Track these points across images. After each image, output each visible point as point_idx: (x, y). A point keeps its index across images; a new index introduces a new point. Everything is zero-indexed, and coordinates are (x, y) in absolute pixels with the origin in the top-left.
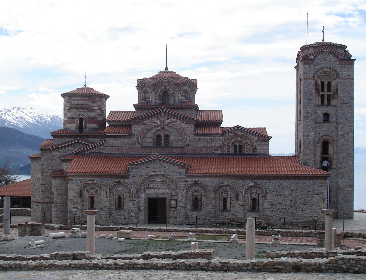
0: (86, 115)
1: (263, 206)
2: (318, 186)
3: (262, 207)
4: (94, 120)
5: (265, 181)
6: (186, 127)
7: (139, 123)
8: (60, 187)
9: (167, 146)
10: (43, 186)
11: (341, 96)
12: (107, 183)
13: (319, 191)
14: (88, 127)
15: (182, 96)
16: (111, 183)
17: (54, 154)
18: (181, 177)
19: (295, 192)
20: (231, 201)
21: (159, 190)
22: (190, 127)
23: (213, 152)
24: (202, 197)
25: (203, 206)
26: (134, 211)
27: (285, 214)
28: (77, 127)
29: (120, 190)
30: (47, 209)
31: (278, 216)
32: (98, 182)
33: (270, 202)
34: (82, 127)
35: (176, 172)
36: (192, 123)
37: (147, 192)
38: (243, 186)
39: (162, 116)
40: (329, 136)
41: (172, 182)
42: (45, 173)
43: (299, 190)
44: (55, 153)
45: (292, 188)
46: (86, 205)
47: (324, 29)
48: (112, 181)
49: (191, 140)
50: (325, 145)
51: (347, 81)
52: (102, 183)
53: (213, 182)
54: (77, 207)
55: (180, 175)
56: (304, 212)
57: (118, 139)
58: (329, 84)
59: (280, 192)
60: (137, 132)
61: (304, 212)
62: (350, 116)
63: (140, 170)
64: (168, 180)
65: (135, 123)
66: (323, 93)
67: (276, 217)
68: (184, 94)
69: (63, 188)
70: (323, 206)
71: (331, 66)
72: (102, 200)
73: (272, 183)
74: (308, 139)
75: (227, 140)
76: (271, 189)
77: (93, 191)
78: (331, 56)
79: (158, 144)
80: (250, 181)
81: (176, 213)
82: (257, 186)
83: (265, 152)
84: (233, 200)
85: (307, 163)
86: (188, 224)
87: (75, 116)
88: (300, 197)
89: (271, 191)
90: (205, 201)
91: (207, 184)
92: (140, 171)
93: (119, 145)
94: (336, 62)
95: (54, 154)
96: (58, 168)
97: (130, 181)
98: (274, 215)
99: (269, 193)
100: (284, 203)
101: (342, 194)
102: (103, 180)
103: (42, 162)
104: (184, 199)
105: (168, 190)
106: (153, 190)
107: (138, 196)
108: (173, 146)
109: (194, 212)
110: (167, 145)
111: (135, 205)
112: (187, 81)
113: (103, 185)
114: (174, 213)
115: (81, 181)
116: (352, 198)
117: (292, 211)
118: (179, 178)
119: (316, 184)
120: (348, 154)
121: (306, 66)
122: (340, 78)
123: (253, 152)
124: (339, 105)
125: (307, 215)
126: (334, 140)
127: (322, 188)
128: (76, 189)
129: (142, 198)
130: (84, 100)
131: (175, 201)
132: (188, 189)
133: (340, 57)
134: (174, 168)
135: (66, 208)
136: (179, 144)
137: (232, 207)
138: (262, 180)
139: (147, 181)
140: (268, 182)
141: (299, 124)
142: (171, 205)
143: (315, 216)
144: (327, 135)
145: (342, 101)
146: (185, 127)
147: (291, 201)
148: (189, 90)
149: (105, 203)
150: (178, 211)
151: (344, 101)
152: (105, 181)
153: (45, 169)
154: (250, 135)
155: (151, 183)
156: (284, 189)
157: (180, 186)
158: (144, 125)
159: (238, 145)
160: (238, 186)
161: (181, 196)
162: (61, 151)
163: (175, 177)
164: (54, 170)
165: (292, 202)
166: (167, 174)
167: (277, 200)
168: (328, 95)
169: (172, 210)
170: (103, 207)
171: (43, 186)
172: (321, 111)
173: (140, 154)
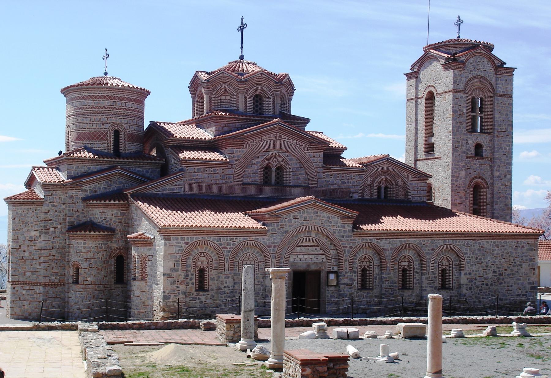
0: (125, 126)
1: (457, 281)
2: (527, 250)
3: (455, 283)
5: (462, 242)
7: (241, 145)
11: (497, 119)
12: (231, 245)
13: (529, 257)
16: (237, 244)
17: (73, 194)
18: (345, 235)
19: (500, 259)
21: (310, 257)
22: (317, 155)
23: (351, 197)
24: (374, 268)
25: (375, 282)
30: (54, 295)
31: (477, 295)
32: (215, 242)
33: (468, 274)
37: (292, 259)
38: (433, 250)
39: (276, 134)
42: (52, 229)
44: (75, 192)
45: (495, 252)
47: (459, 20)
50: (476, 189)
51: (505, 98)
52: (221, 244)
53: (391, 243)
54: (178, 289)
55: (345, 232)
57: (205, 169)
59: (480, 259)
60: (236, 158)
61: (510, 288)
62: (508, 149)
63: (284, 222)
64: (324, 240)
67: (476, 297)
69: (100, 255)
70: (533, 279)
72: (221, 275)
74: (458, 181)
75: (370, 178)
76: (470, 255)
78: (486, 60)
79: (266, 181)
80: (442, 242)
81: (335, 295)
83: (421, 199)
84: (417, 272)
87: (107, 126)
89: (469, 257)
91: (384, 246)
92: (283, 223)
93: (207, 181)
94: (491, 70)
95: (73, 193)
97: (268, 242)
98: (473, 295)
99: (467, 260)
100: (485, 276)
102: (223, 239)
103: (44, 208)
104: (350, 272)
105: (324, 256)
106: (301, 256)
108: (291, 184)
109: (362, 293)
110: (278, 183)
113: (223, 248)
114: (333, 294)
115: (186, 241)
117: (495, 288)
118: (343, 236)
119: (525, 246)
123: (405, 198)
124: (496, 133)
125: (514, 292)
128: (176, 256)
131: (335, 275)
134: (336, 219)
135: (104, 293)
136: (300, 182)
137: (416, 284)
138: (458, 241)
139: (292, 241)
140: (466, 243)
142: (329, 281)
143: (523, 294)
145: (500, 127)
146: (310, 154)
147: (494, 272)
148: (286, 94)
150: (341, 292)
151: (501, 127)
152: (226, 241)
154: (403, 172)
155: (299, 246)
156: (486, 254)
157: (344, 250)
158: (248, 148)
159: (383, 186)
162: (86, 189)
163: (337, 235)
164: (72, 222)
165: (495, 274)
166: (326, 230)
167: (476, 271)
169: (330, 290)
170: (222, 287)
172: (472, 140)
173: (240, 197)
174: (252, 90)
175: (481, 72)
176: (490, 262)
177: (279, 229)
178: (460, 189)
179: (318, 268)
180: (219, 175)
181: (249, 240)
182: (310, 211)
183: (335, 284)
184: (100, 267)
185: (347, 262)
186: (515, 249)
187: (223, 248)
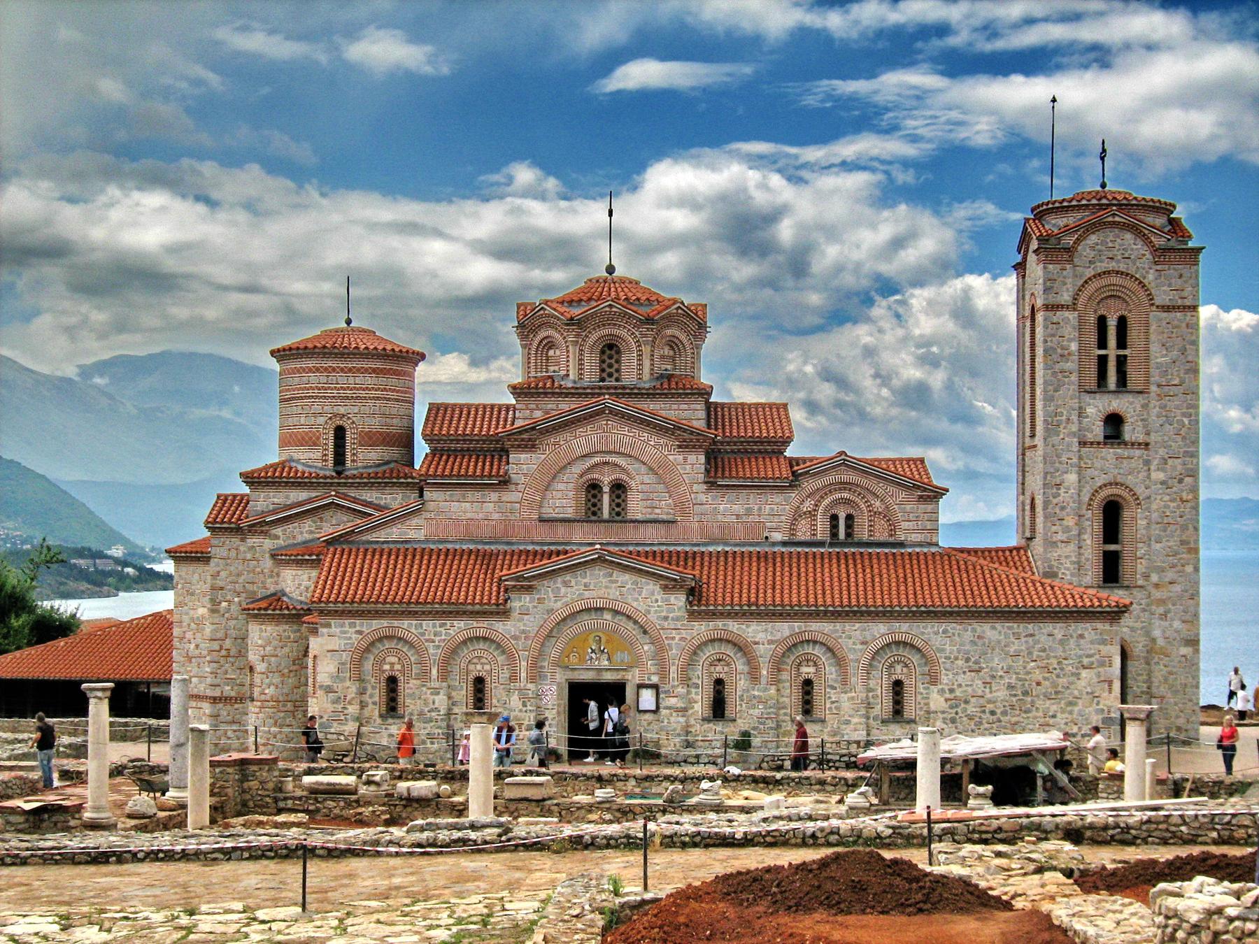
2: (1092, 642)
4: (381, 434)
5: (933, 627)
6: (681, 457)
7: (533, 446)
8: (275, 648)
9: (619, 518)
10: (216, 646)
11: (1158, 360)
13: (1097, 656)
14: (362, 457)
15: (662, 357)
18: (671, 615)
20: (828, 690)
22: (692, 458)
23: (767, 538)
25: (741, 705)
26: (526, 723)
27: (992, 728)
28: (325, 455)
29: (479, 658)
30: (230, 718)
32: (413, 630)
34: (344, 455)
35: (657, 601)
36: (700, 447)
38: (863, 643)
40: (1122, 485)
41: (645, 632)
43: (1036, 653)
45: (1012, 650)
46: (374, 703)
48: (458, 628)
49: (696, 498)
51: (1178, 314)
52: (423, 634)
54: (346, 712)
56: (1051, 721)
58: (1122, 323)
59: (976, 662)
62: (1187, 423)
64: (630, 625)
65: (519, 446)
66: (1102, 352)
68: (667, 351)
69: (287, 650)
71: (1128, 269)
72: (424, 689)
73: (954, 635)
74: (1059, 495)
77: (394, 660)
78: (1128, 236)
79: (591, 513)
82: (905, 644)
84: (834, 688)
85: (1055, 569)
86: (694, 760)
87: (321, 420)
88: (1038, 676)
90: (748, 691)
93: (469, 515)
94: (1144, 255)
95: (252, 541)
96: (268, 586)
99: (944, 663)
100: (988, 696)
101: (1162, 667)
102: (427, 625)
103: (213, 566)
107: (536, 675)
108: (640, 517)
110: (618, 514)
111: (528, 704)
112: (680, 311)
113: (427, 641)
115: (358, 628)
116: (1193, 678)
117: (1014, 720)
118: (666, 618)
120: (1183, 542)
121: (1051, 266)
122: (1157, 304)
124: (1153, 388)
126: (1138, 499)
127: (1105, 649)
129: (548, 682)
130: (350, 370)
131: (654, 691)
132: (695, 653)
133: (1159, 242)
134: (651, 588)
136: (657, 511)
141: (1030, 448)
144: (1117, 484)
147: (1010, 687)
148: (683, 337)
149: (432, 697)
153: (222, 589)
158: (547, 452)
160: (851, 641)
161: (673, 675)
163: (652, 617)
164: (254, 593)
167: (967, 685)
168: (1118, 357)
170: (426, 709)
171: (216, 646)
172: (1097, 407)
174: (594, 337)
175: (1118, 262)
176: (1000, 667)
177: (535, 607)
178: (1064, 513)
179: (619, 677)
180: (492, 505)
181: (475, 624)
182: (597, 572)
183: (653, 708)
184: (286, 671)
185: (675, 667)
186: (1061, 642)
187: (427, 641)
